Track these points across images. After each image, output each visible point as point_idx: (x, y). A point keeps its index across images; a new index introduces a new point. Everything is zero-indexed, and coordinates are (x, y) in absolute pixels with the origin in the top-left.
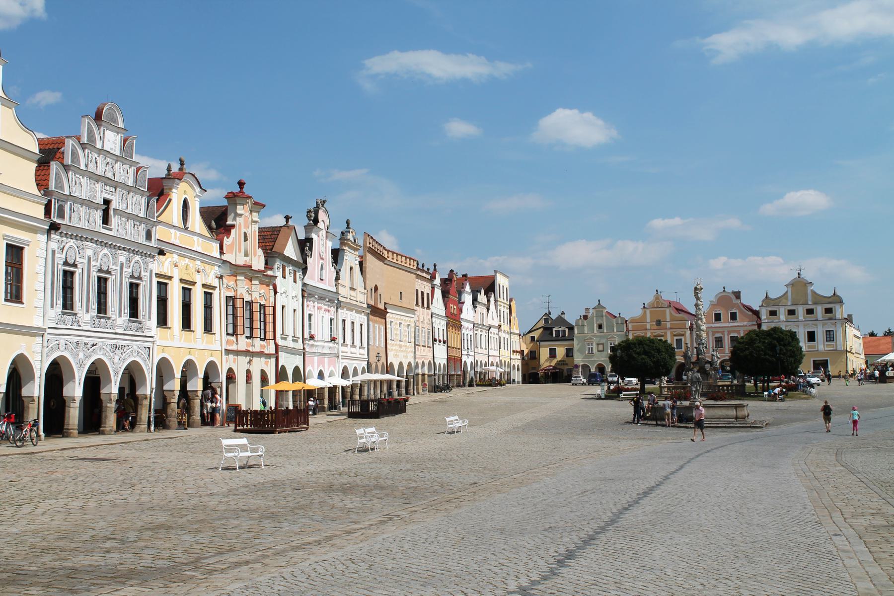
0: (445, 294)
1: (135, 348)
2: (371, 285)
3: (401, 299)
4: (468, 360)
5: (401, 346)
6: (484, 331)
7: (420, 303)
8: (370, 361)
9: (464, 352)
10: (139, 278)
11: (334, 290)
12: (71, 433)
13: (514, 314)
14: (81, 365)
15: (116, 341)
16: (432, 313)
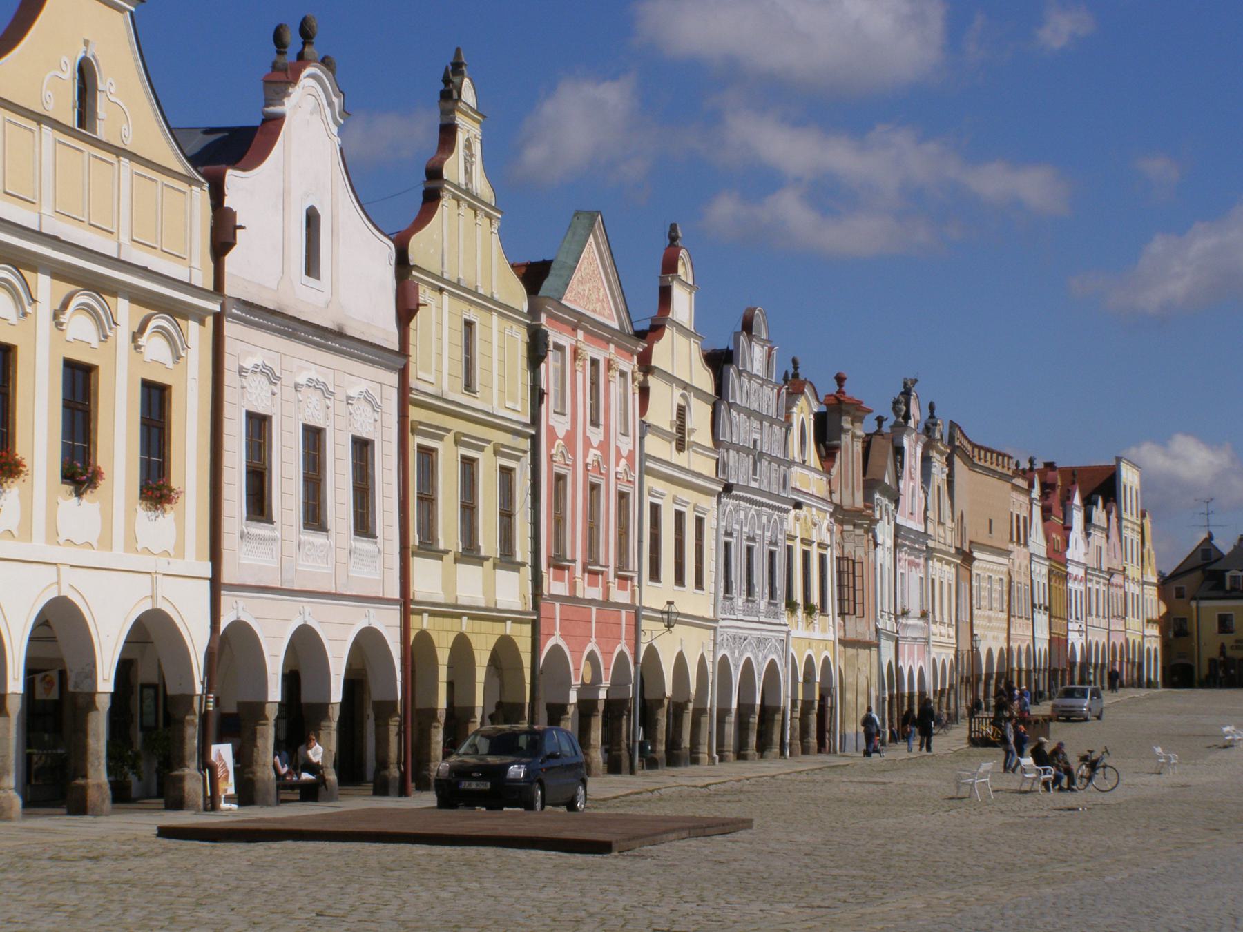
0: (1046, 512)
1: (774, 640)
2: (957, 515)
3: (990, 532)
4: (1076, 641)
5: (990, 619)
6: (1102, 580)
7: (1015, 539)
8: (960, 649)
9: (1071, 626)
10: (776, 544)
11: (921, 528)
12: (727, 756)
13: (1148, 544)
14: (737, 666)
15: (759, 633)
16: (1031, 554)
